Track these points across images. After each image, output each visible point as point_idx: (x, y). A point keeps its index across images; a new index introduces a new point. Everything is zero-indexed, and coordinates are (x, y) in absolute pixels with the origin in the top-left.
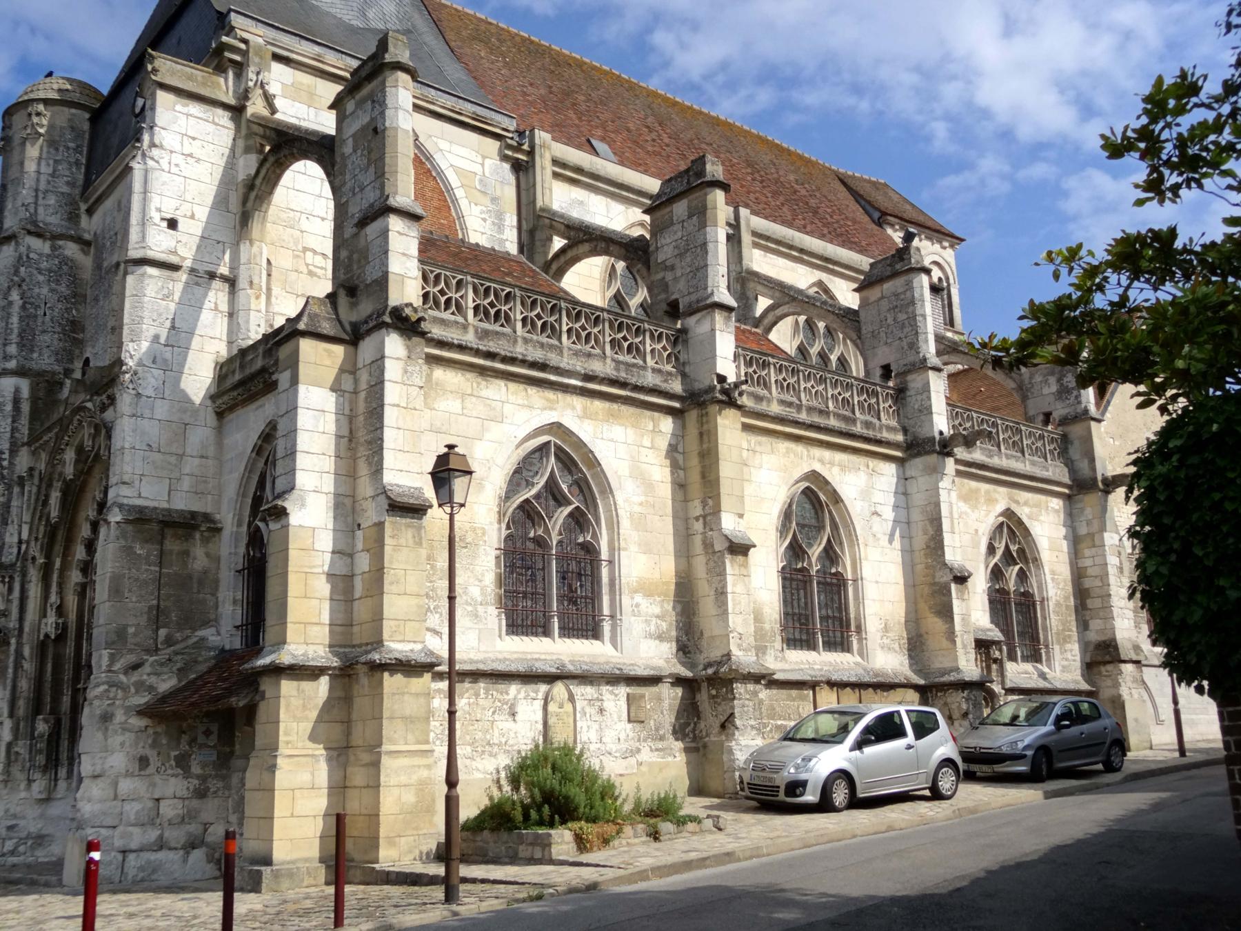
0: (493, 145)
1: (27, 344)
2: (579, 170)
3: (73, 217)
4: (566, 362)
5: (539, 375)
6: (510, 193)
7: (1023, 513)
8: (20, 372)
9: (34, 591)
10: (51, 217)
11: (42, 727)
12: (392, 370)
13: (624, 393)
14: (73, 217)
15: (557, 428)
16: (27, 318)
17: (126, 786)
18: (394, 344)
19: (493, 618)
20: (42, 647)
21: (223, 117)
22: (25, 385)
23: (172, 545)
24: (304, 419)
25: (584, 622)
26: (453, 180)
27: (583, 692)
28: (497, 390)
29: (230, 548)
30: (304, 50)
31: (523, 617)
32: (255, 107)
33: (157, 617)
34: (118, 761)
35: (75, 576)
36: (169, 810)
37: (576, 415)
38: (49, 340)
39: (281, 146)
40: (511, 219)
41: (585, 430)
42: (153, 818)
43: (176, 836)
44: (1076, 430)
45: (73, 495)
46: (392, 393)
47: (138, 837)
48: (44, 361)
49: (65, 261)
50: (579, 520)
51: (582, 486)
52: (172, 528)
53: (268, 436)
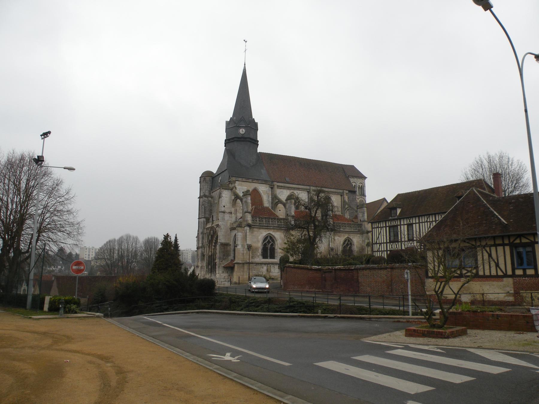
0: (268, 186)
1: (205, 214)
2: (282, 186)
3: (210, 194)
4: (271, 225)
5: (267, 228)
6: (270, 192)
7: (351, 237)
8: (204, 218)
9: (208, 249)
10: (207, 194)
11: (210, 267)
12: (248, 231)
13: (279, 228)
14: (210, 194)
15: (269, 233)
16: (205, 210)
17: (222, 275)
18: (247, 228)
19: (261, 257)
20: (209, 257)
21: (230, 191)
22: (205, 219)
23: (226, 247)
24: (239, 236)
25: (273, 256)
26: (261, 192)
27: (272, 266)
28: (261, 230)
29: (232, 247)
30: (240, 179)
31: (265, 256)
32: (234, 189)
33: (224, 255)
34: (220, 272)
35: (213, 247)
36: (226, 277)
37: (272, 232)
38: (207, 213)
39: (237, 197)
40: (270, 196)
41: (273, 233)
42: (224, 278)
43: (227, 280)
44: (363, 223)
45: (212, 237)
46: (248, 234)
47: (223, 280)
48: (207, 216)
49: (209, 201)
50: (272, 245)
51: (273, 241)
52: (225, 245)
53: (235, 235)
